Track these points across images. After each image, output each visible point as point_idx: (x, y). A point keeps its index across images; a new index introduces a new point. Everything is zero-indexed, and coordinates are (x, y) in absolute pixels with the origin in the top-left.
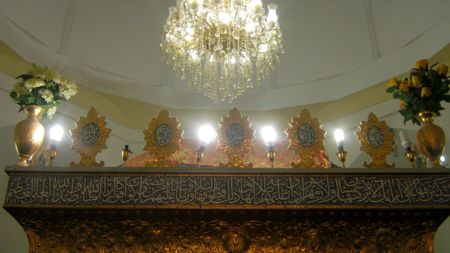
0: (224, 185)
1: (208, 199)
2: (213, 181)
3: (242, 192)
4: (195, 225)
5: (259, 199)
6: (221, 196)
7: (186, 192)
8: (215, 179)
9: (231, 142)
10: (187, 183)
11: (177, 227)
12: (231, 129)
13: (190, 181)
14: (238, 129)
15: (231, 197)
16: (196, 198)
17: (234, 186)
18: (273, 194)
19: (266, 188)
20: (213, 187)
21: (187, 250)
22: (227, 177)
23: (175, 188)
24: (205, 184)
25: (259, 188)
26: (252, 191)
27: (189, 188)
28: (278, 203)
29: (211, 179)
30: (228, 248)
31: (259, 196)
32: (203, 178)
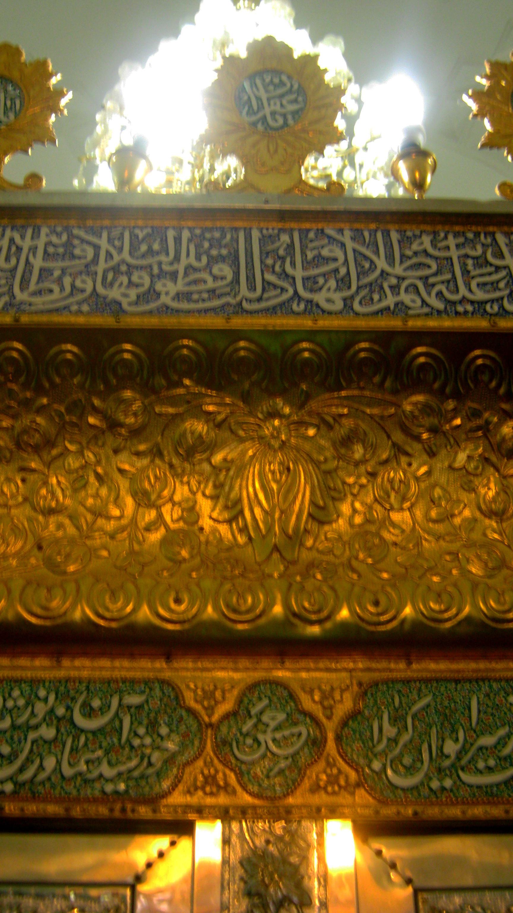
0: (224, 252)
1: (151, 294)
2: (178, 240)
3: (299, 274)
4: (96, 410)
5: (376, 297)
6: (211, 284)
7: (57, 273)
8: (186, 235)
9: (254, 118)
10: (69, 245)
11: (15, 417)
12: (254, 85)
13: (78, 237)
14: (282, 84)
15: (252, 288)
16: (100, 289)
17: (265, 254)
18: (431, 280)
19: (401, 262)
20: (177, 258)
21: (53, 520)
22: (236, 229)
23: (13, 261)
24: (144, 248)
25: (372, 262)
26: (343, 271)
27: (73, 257)
28: (460, 309)
29: (171, 234)
30: (241, 512)
31: (376, 287)
32: (137, 231)
